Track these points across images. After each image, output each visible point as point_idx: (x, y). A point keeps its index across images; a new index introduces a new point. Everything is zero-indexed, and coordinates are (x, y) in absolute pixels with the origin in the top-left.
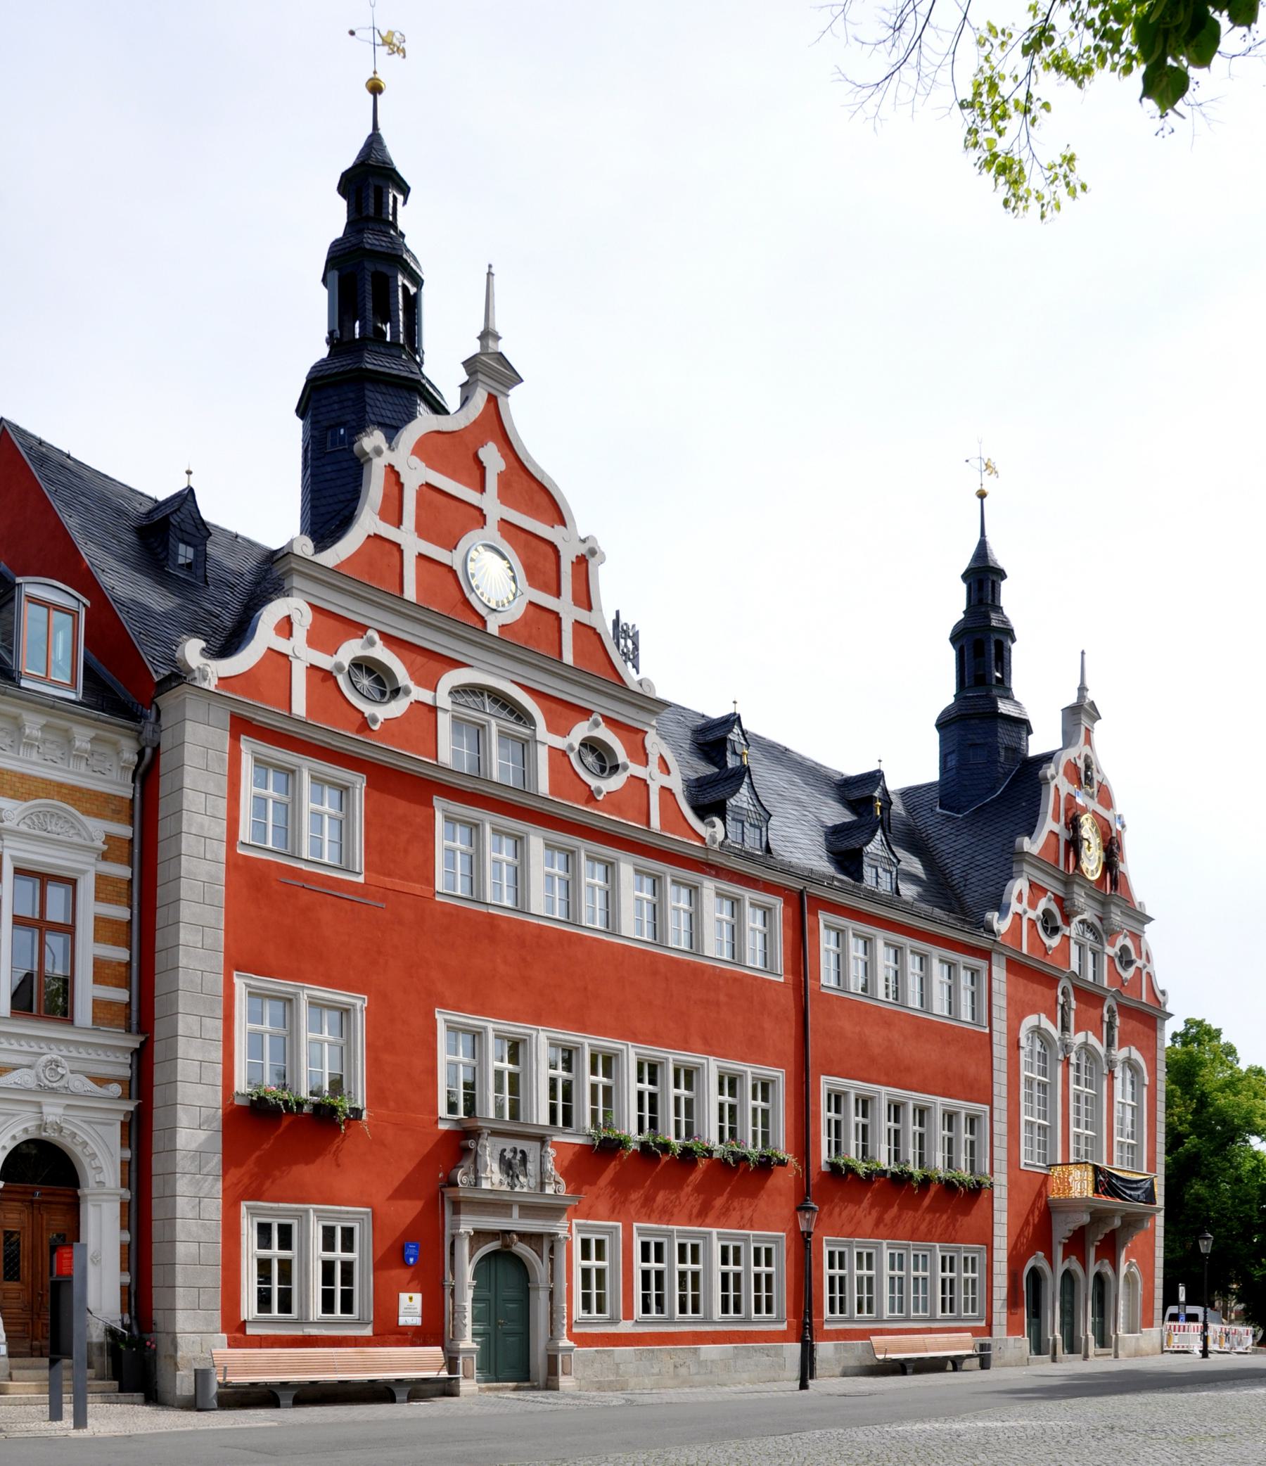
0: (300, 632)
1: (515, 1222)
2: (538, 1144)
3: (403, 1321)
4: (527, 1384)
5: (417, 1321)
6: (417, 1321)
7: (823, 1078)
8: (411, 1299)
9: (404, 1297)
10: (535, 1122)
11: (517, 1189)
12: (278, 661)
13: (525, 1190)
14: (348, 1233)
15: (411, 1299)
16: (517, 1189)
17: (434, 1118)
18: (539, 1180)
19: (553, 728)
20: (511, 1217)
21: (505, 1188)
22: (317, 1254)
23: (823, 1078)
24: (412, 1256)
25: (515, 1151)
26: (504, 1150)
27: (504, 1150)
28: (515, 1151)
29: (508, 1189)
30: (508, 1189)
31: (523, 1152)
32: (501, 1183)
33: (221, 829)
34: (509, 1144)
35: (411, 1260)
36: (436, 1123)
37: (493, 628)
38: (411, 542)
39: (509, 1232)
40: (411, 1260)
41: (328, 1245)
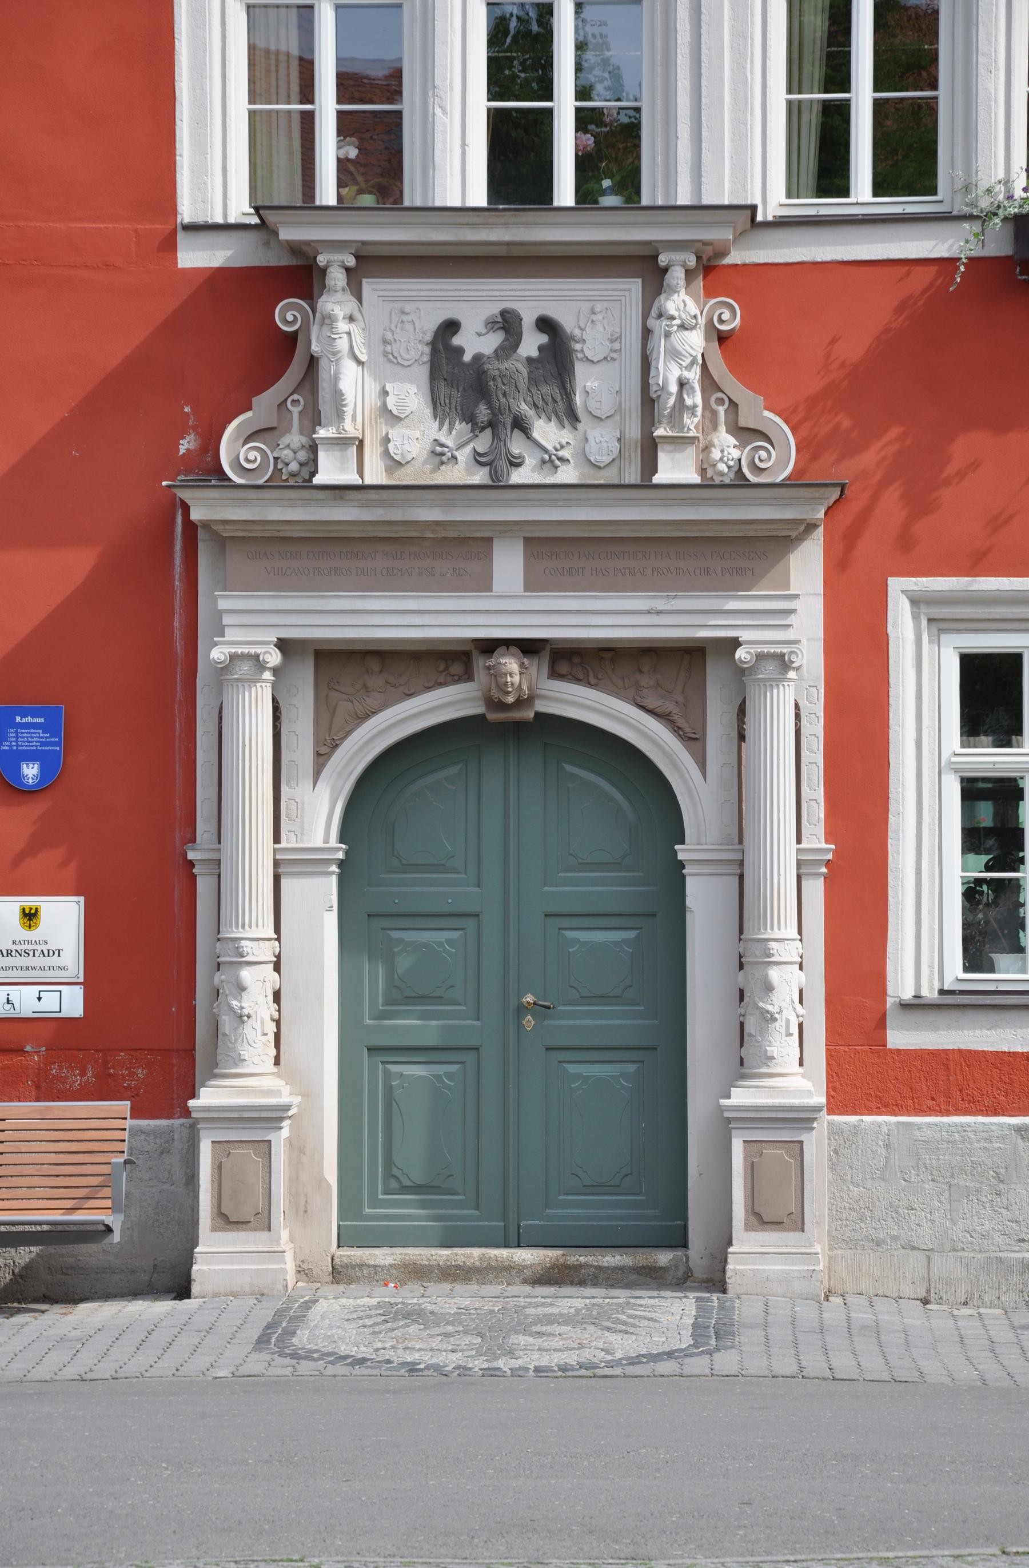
2: (633, 288)
4: (663, 1258)
8: (30, 916)
10: (684, 199)
11: (518, 477)
13: (567, 475)
15: (30, 916)
16: (518, 477)
17: (161, 228)
18: (634, 431)
20: (484, 584)
24: (30, 757)
26: (451, 327)
27: (451, 327)
29: (480, 477)
30: (480, 477)
31: (545, 324)
32: (439, 456)
35: (30, 771)
36: (169, 245)
39: (489, 646)
40: (30, 771)
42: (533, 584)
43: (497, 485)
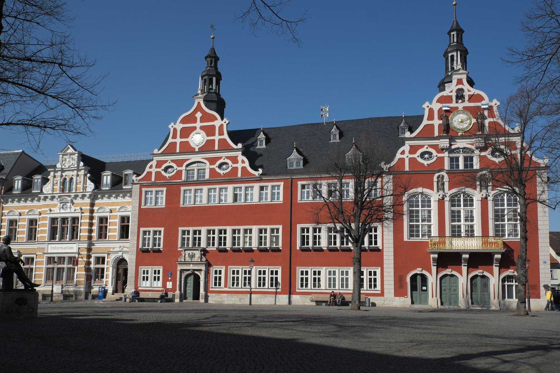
0: (154, 166)
1: (191, 267)
3: (167, 287)
5: (171, 287)
6: (171, 287)
7: (298, 225)
9: (168, 283)
12: (150, 173)
14: (159, 271)
19: (211, 164)
21: (199, 260)
22: (149, 275)
23: (298, 225)
25: (192, 253)
26: (189, 253)
27: (189, 253)
28: (192, 253)
33: (138, 205)
34: (190, 252)
37: (197, 150)
38: (178, 140)
41: (144, 273)
42: (193, 266)
43: (192, 262)
